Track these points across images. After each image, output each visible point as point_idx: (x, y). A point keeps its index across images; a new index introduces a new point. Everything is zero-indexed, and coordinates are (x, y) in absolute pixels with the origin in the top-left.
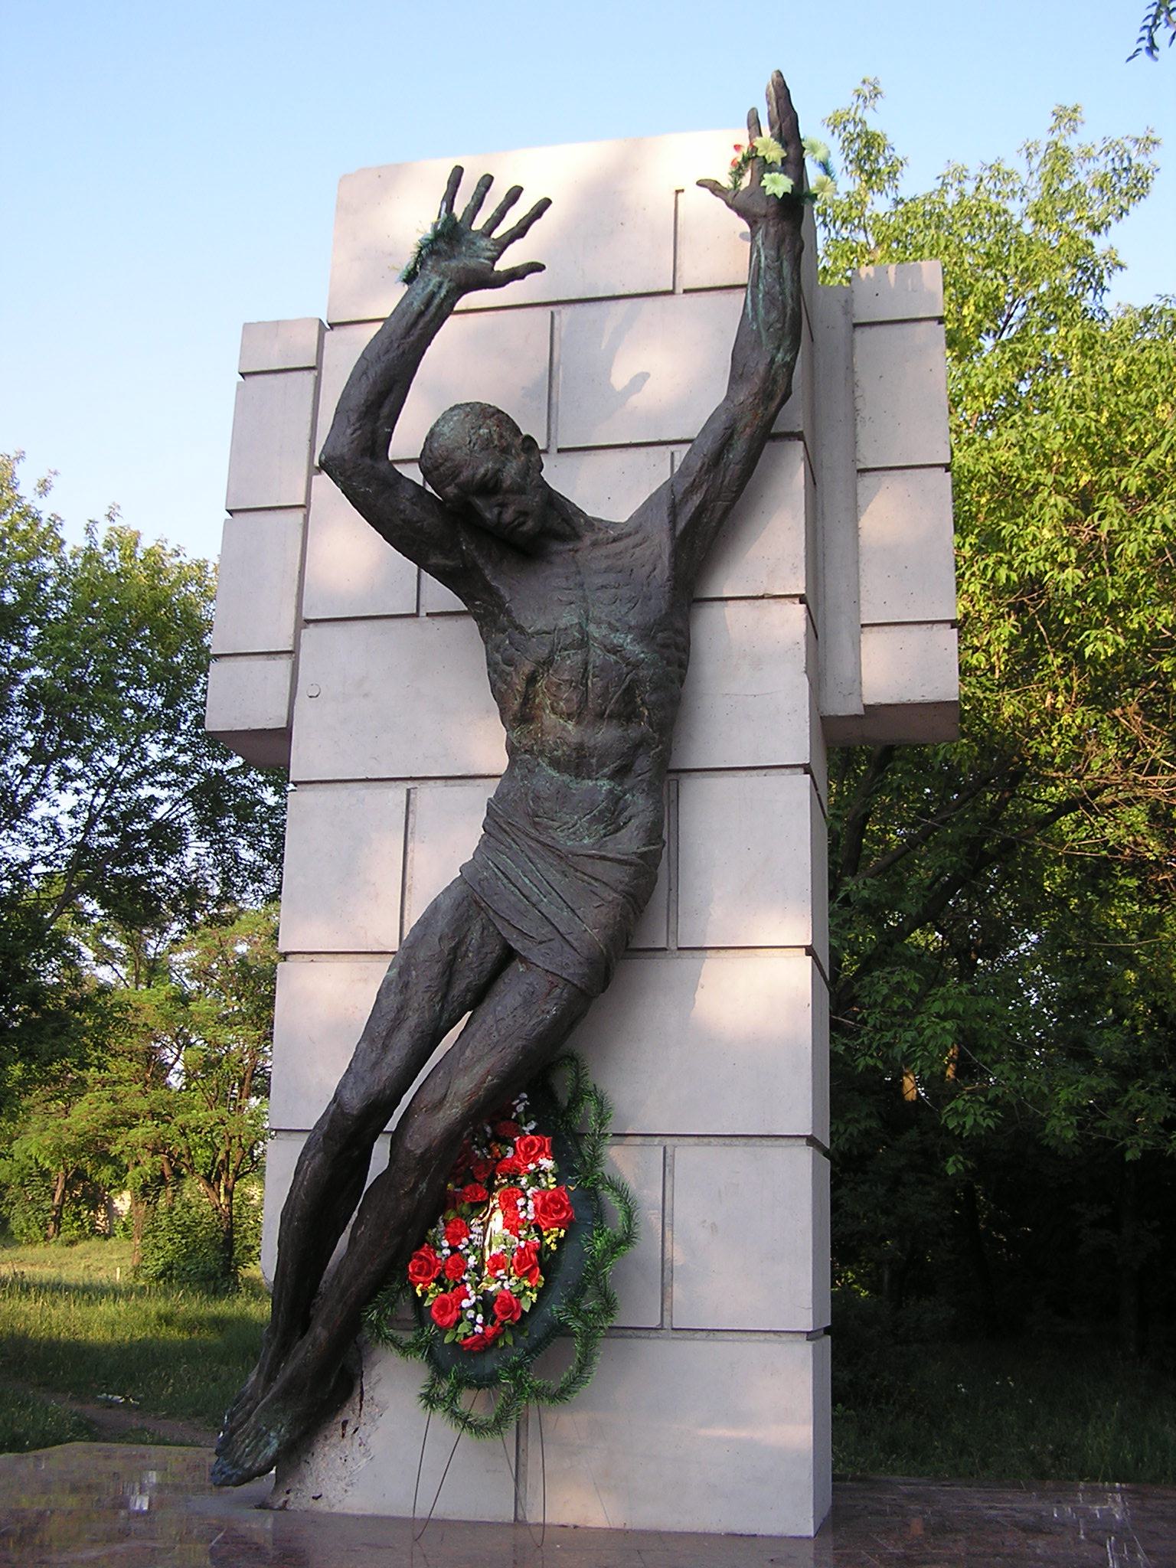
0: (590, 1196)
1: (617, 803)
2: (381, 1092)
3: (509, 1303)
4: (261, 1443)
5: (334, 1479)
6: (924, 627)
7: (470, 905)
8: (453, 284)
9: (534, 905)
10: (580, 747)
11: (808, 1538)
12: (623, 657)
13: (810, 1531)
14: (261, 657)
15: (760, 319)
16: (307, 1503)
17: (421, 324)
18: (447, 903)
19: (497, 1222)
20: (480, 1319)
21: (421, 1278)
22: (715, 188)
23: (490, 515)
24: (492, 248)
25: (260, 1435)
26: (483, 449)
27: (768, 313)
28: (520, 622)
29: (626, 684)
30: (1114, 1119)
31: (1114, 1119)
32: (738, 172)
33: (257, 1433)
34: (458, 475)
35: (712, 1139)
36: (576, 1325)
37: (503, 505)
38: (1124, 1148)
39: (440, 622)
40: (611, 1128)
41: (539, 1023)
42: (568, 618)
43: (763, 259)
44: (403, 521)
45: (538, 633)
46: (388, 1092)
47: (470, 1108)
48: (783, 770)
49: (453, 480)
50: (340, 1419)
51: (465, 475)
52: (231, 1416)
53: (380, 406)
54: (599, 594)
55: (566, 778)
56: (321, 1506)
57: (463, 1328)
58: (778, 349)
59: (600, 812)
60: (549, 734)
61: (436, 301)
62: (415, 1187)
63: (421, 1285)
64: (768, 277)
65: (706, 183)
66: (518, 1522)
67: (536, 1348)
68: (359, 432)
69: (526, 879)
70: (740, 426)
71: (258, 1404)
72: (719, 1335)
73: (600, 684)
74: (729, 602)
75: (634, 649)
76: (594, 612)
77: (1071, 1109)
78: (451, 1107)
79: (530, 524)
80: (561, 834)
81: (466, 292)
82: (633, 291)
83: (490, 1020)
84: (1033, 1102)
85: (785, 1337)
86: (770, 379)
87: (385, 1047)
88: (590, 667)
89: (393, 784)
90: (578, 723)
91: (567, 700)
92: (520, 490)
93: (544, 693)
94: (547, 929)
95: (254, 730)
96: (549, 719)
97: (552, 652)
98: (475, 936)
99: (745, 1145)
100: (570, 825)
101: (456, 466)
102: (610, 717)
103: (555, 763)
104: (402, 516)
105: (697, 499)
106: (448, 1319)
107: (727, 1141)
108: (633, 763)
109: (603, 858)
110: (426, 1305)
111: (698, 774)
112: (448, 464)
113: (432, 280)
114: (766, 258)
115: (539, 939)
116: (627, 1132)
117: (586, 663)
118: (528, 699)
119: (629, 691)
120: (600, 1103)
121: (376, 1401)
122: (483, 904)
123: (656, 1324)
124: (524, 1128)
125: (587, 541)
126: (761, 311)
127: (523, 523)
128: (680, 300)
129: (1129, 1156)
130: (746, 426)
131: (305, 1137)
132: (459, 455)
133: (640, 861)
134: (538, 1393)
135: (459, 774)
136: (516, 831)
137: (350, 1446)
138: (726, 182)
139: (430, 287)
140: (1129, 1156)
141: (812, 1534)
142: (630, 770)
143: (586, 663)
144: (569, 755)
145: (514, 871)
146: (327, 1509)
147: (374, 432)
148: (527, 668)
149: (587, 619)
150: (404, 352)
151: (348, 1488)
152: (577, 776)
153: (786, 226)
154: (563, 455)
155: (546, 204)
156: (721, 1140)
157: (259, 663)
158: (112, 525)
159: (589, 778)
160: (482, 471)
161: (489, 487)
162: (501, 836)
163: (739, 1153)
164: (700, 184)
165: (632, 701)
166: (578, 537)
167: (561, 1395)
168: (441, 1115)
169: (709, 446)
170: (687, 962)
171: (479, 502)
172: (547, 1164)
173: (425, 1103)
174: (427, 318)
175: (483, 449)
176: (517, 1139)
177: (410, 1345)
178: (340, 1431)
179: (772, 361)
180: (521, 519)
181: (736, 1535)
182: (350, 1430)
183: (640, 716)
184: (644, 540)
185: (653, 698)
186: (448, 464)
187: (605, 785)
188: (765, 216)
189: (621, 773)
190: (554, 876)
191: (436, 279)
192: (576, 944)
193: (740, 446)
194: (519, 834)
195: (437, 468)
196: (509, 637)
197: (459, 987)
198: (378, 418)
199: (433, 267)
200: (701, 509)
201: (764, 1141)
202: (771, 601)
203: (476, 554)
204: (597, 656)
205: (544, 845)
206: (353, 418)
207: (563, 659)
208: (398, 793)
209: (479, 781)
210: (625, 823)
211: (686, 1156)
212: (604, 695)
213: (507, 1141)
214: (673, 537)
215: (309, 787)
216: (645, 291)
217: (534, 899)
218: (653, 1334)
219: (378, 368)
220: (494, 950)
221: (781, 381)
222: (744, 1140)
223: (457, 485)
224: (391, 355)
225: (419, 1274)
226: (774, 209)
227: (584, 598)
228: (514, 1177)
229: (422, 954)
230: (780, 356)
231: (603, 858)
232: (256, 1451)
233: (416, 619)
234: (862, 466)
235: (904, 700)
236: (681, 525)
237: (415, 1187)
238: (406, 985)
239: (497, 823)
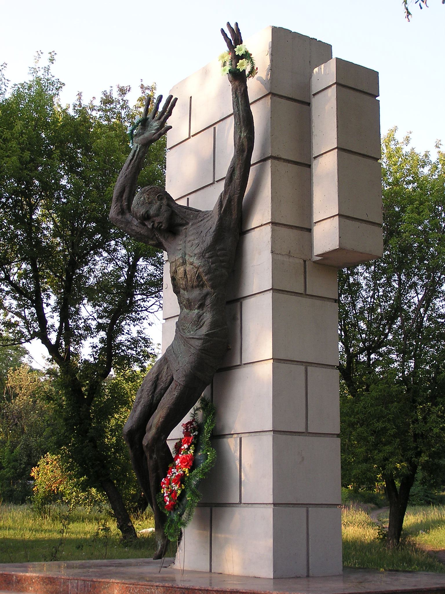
1: (199, 317)
2: (132, 427)
7: (164, 360)
8: (141, 145)
11: (271, 579)
17: (132, 163)
24: (157, 125)
26: (142, 205)
29: (197, 275)
35: (252, 434)
37: (153, 222)
41: (172, 399)
46: (134, 426)
47: (158, 429)
53: (122, 196)
55: (188, 311)
58: (241, 132)
62: (151, 457)
70: (236, 164)
72: (254, 505)
74: (256, 229)
75: (197, 262)
76: (187, 252)
79: (164, 225)
87: (135, 411)
90: (187, 291)
92: (157, 215)
96: (182, 291)
97: (175, 268)
98: (165, 370)
102: (195, 287)
105: (227, 196)
108: (205, 302)
111: (248, 298)
117: (185, 271)
118: (176, 286)
119: (199, 277)
123: (238, 501)
124: (192, 434)
125: (190, 224)
127: (162, 226)
133: (206, 337)
142: (204, 304)
143: (185, 271)
147: (121, 206)
149: (185, 254)
150: (126, 175)
152: (191, 310)
153: (237, 83)
154: (218, 183)
155: (176, 99)
158: (439, 150)
160: (141, 213)
165: (202, 280)
166: (187, 223)
174: (133, 161)
175: (142, 205)
179: (240, 137)
180: (160, 225)
184: (211, 218)
185: (206, 278)
187: (196, 311)
189: (201, 306)
193: (237, 173)
198: (122, 201)
200: (230, 201)
201: (264, 434)
202: (265, 226)
210: (203, 324)
214: (220, 214)
218: (237, 505)
221: (246, 144)
224: (123, 178)
227: (185, 247)
230: (242, 134)
231: (193, 338)
234: (314, 156)
235: (324, 252)
237: (151, 457)
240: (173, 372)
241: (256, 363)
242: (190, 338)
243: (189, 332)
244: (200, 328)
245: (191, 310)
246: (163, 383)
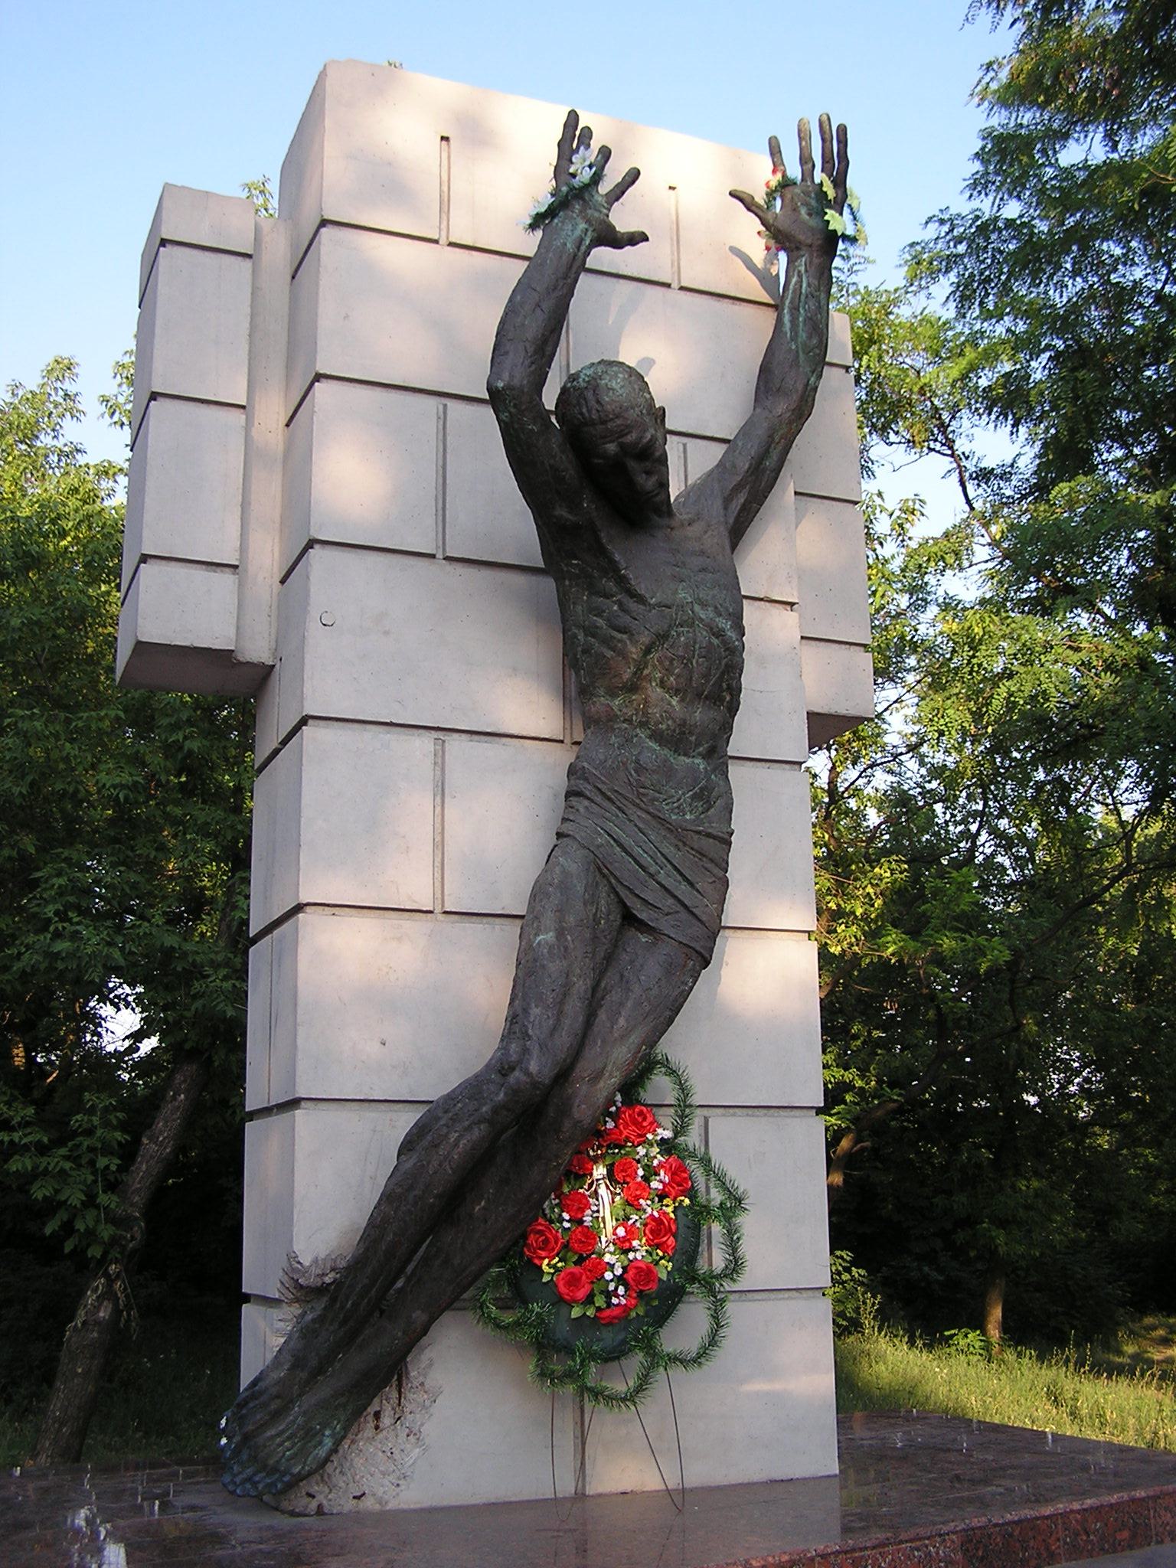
4: (313, 1443)
5: (378, 1475)
6: (843, 646)
9: (651, 876)
10: (685, 721)
11: (836, 1476)
12: (724, 643)
13: (835, 1468)
14: (199, 566)
15: (800, 340)
16: (349, 1505)
20: (621, 1290)
21: (543, 1254)
22: (749, 204)
25: (310, 1435)
27: (810, 337)
28: (641, 589)
32: (771, 195)
33: (307, 1434)
34: (626, 434)
35: (737, 1110)
39: (460, 569)
40: (696, 1100)
43: (804, 285)
44: (551, 466)
45: (659, 605)
48: (784, 766)
49: (618, 438)
50: (371, 1410)
51: (630, 438)
52: (239, 1419)
54: (701, 575)
55: (666, 751)
56: (369, 1504)
57: (600, 1301)
59: (701, 789)
60: (656, 706)
61: (583, 248)
63: (546, 1261)
64: (811, 303)
65: (741, 195)
66: (580, 1496)
68: (533, 367)
69: (639, 850)
70: (777, 439)
71: (292, 1401)
72: (750, 1295)
73: (706, 664)
78: (611, 1076)
80: (667, 808)
81: (606, 245)
82: (635, 274)
83: (637, 990)
85: (805, 1294)
88: (697, 646)
89: (415, 731)
90: (682, 700)
91: (678, 676)
93: (654, 666)
94: (671, 901)
95: (196, 648)
96: (655, 692)
99: (765, 1115)
100: (675, 799)
101: (627, 426)
103: (657, 736)
104: (552, 462)
105: (741, 498)
106: (581, 1294)
107: (750, 1111)
109: (709, 835)
110: (544, 1280)
112: (619, 422)
114: (809, 285)
115: (666, 910)
116: (666, 1103)
120: (672, 1072)
121: (427, 1387)
122: (605, 871)
126: (803, 335)
128: (674, 294)
130: (781, 438)
131: (425, 1108)
132: (633, 414)
134: (675, 1359)
135: (489, 730)
136: (623, 800)
137: (392, 1437)
138: (760, 198)
139: (578, 233)
141: (837, 1472)
144: (674, 731)
145: (628, 842)
146: (377, 1507)
148: (645, 639)
151: (400, 1482)
152: (675, 752)
156: (745, 1111)
157: (199, 574)
159: (686, 755)
162: (606, 804)
164: (733, 194)
167: (697, 1359)
168: (601, 1084)
169: (753, 448)
171: (632, 464)
173: (589, 1072)
176: (613, 1109)
177: (517, 1324)
178: (371, 1424)
181: (776, 1481)
182: (386, 1420)
183: (722, 700)
186: (619, 422)
188: (810, 246)
190: (669, 850)
191: (583, 226)
192: (704, 918)
194: (626, 803)
195: (604, 422)
196: (620, 604)
197: (601, 953)
199: (581, 212)
201: (782, 1112)
203: (595, 514)
204: (703, 636)
205: (654, 816)
206: (531, 350)
207: (678, 635)
208: (424, 743)
209: (504, 740)
212: (706, 676)
215: (322, 723)
216: (647, 277)
217: (652, 870)
219: (548, 305)
222: (765, 1111)
223: (622, 446)
225: (540, 1249)
226: (820, 242)
229: (571, 919)
231: (709, 835)
233: (432, 560)
235: (832, 711)
236: (731, 521)
238: (566, 948)
240: (643, 915)
241: (747, 932)
242: (699, 833)
243: (680, 810)
244: (708, 810)
245: (675, 752)
246: (605, 937)
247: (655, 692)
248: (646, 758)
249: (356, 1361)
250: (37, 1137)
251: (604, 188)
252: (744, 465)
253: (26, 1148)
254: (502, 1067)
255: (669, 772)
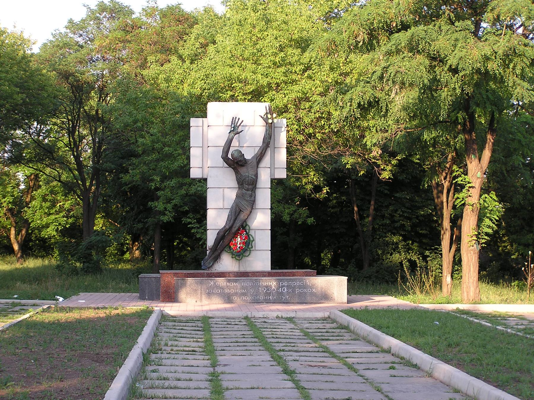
0: (249, 236)
3: (242, 247)
18: (234, 205)
19: (239, 239)
22: (261, 117)
23: (240, 164)
25: (210, 263)
30: (296, 215)
31: (296, 215)
36: (248, 249)
38: (298, 221)
42: (247, 174)
67: (244, 252)
77: (288, 214)
84: (281, 213)
86: (268, 143)
96: (245, 185)
103: (245, 190)
113: (232, 134)
129: (299, 223)
134: (245, 256)
137: (219, 264)
138: (263, 117)
140: (299, 223)
161: (240, 161)
163: (262, 231)
170: (257, 210)
172: (245, 233)
193: (264, 151)
208: (222, 190)
211: (257, 231)
213: (239, 230)
220: (239, 210)
228: (241, 234)
232: (209, 265)
239: (237, 196)
247: (245, 185)
248: (244, 192)
249: (213, 256)
250: (196, 226)
251: (238, 125)
252: (259, 153)
253: (195, 228)
254: (225, 227)
255: (246, 194)
